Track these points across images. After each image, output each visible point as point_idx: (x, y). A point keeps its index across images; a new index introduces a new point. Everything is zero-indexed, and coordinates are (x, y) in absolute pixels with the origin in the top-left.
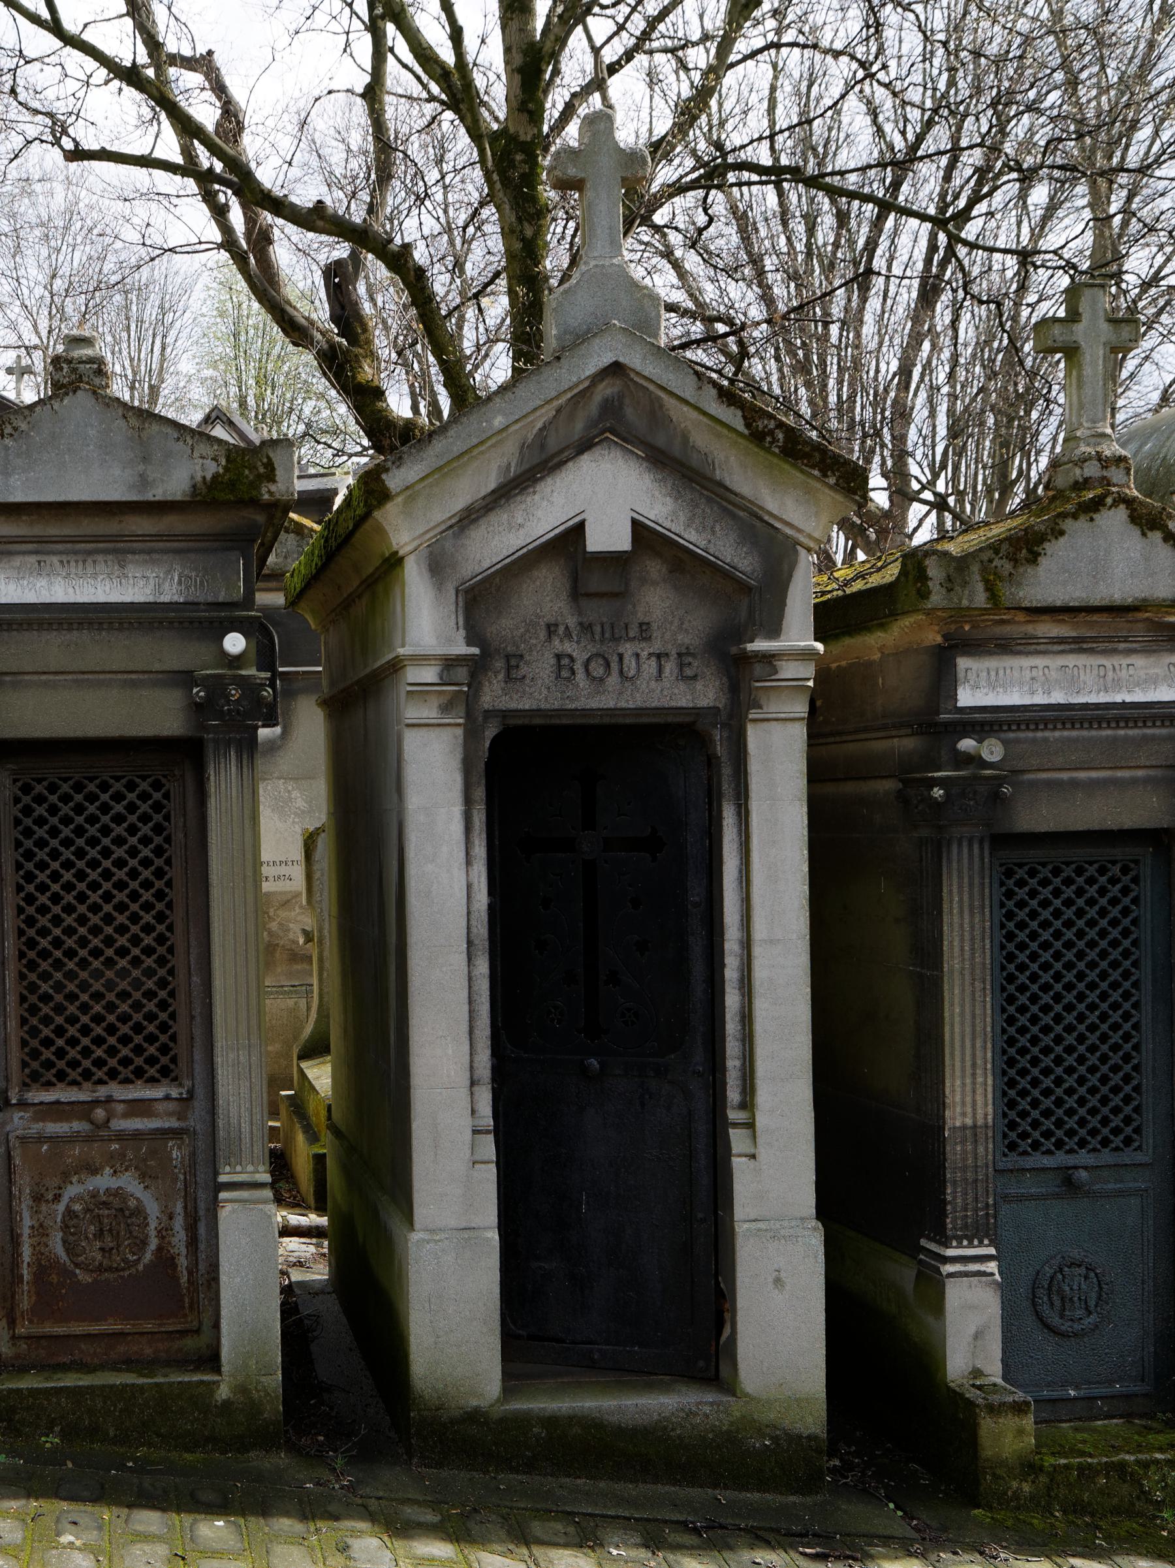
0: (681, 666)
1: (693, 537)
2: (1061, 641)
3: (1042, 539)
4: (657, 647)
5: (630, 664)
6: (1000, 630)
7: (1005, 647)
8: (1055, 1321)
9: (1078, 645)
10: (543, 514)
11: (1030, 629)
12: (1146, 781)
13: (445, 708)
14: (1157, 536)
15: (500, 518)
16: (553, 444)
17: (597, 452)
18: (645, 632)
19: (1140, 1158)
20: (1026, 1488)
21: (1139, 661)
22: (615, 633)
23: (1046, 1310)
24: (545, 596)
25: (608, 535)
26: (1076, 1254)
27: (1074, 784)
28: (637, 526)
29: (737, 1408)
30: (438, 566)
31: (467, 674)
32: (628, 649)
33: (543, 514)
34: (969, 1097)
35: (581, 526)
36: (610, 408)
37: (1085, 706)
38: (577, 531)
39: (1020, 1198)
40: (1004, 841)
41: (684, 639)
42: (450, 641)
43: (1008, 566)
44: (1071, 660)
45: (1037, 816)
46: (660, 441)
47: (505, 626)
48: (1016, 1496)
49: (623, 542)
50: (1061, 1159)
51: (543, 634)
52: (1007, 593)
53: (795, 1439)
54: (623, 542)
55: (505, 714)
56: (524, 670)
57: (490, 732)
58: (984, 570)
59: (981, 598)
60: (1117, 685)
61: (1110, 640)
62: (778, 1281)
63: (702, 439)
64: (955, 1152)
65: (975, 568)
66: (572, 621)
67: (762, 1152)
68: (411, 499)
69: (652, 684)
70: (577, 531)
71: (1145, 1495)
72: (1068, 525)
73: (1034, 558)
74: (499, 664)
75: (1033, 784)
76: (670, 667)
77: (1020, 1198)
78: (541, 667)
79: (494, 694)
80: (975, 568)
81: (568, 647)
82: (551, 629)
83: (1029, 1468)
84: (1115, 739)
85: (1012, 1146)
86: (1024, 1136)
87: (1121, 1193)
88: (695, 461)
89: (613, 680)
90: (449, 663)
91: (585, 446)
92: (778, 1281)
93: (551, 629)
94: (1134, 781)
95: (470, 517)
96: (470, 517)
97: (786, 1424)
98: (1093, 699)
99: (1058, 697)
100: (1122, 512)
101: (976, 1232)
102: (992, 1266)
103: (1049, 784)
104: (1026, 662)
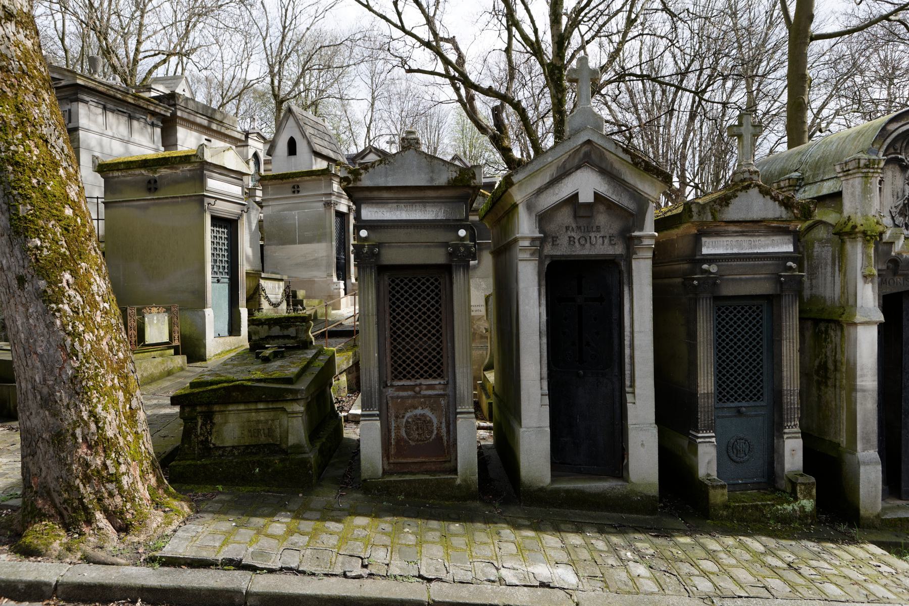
0: (610, 240)
1: (614, 198)
2: (736, 232)
3: (730, 198)
4: (602, 234)
5: (593, 240)
6: (716, 229)
7: (718, 234)
8: (735, 458)
9: (742, 234)
10: (565, 190)
11: (726, 228)
12: (765, 278)
13: (532, 254)
14: (768, 197)
15: (550, 191)
16: (568, 167)
17: (582, 169)
18: (598, 229)
19: (762, 403)
20: (725, 513)
21: (762, 239)
22: (588, 229)
23: (731, 454)
24: (565, 217)
25: (586, 197)
26: (741, 435)
27: (741, 279)
28: (596, 195)
29: (629, 487)
30: (529, 207)
31: (539, 243)
32: (593, 235)
33: (565, 190)
34: (706, 384)
35: (577, 194)
36: (587, 155)
37: (745, 254)
38: (576, 196)
39: (723, 417)
40: (717, 298)
41: (611, 231)
42: (534, 232)
43: (719, 207)
44: (740, 239)
45: (728, 290)
46: (603, 166)
47: (552, 227)
48: (721, 516)
49: (591, 199)
50: (736, 404)
51: (564, 230)
52: (720, 217)
53: (648, 497)
54: (591, 199)
55: (552, 256)
56: (558, 242)
57: (547, 263)
58: (711, 209)
59: (710, 218)
60: (755, 247)
61: (752, 232)
62: (642, 445)
63: (617, 165)
64: (701, 402)
65: (708, 208)
66: (574, 226)
67: (637, 402)
68: (521, 185)
69: (601, 246)
70: (576, 196)
71: (764, 516)
72: (739, 193)
73: (727, 205)
74: (550, 240)
75: (728, 279)
76: (606, 241)
77: (723, 417)
78: (564, 241)
79: (548, 250)
80: (708, 208)
81: (573, 234)
82: (567, 228)
83: (726, 506)
84: (754, 265)
85: (720, 400)
86: (724, 396)
87: (756, 415)
88: (615, 172)
89: (588, 245)
90: (533, 239)
91: (578, 167)
92: (642, 445)
93: (567, 228)
94: (761, 279)
95: (540, 191)
96: (540, 191)
97: (645, 492)
98: (747, 251)
99: (735, 251)
100: (757, 189)
101: (708, 428)
102: (714, 440)
103: (732, 279)
104: (725, 239)
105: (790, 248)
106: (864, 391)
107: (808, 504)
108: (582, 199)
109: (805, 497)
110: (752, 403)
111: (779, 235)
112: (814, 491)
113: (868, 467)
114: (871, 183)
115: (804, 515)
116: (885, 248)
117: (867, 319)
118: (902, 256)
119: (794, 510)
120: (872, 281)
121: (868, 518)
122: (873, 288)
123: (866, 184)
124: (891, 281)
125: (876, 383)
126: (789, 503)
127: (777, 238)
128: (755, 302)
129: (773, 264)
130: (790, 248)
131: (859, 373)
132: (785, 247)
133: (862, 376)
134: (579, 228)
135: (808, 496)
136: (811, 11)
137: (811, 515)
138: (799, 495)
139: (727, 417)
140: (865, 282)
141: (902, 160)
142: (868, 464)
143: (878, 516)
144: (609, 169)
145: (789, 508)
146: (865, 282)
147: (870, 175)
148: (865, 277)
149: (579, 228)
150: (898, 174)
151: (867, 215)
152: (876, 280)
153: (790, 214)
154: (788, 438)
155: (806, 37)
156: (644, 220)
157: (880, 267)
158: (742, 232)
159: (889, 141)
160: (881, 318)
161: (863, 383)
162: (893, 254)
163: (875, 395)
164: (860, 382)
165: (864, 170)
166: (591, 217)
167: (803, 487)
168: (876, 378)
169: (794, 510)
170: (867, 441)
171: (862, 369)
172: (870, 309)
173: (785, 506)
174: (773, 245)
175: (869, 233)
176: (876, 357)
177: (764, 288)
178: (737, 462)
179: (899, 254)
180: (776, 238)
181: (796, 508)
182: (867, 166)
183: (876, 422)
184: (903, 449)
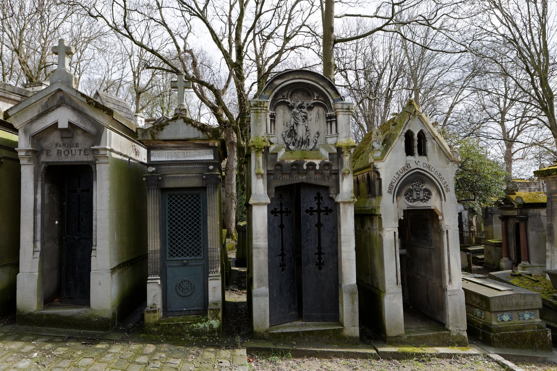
0: (85, 152)
1: (81, 125)
2: (174, 147)
3: (164, 125)
4: (79, 148)
5: (74, 152)
6: (159, 145)
7: (162, 148)
8: (181, 293)
9: (178, 148)
10: (49, 120)
11: (166, 145)
12: (195, 177)
13: (29, 161)
14: (190, 125)
15: (40, 121)
16: (50, 106)
17: (61, 108)
18: (77, 145)
19: (200, 258)
20: (156, 329)
21: (192, 151)
22: (71, 146)
23: (178, 291)
24: (55, 138)
25: (63, 125)
26: (186, 279)
27: (178, 177)
28: (70, 123)
30: (26, 132)
31: (35, 153)
32: (73, 149)
33: (49, 120)
34: (154, 244)
35: (57, 123)
36: (62, 98)
37: (180, 161)
38: (56, 124)
39: (172, 267)
40: (164, 190)
41: (86, 147)
42: (28, 147)
43: (156, 131)
44: (177, 151)
45: (169, 184)
46: (73, 105)
47: (46, 144)
48: (153, 331)
49: (66, 126)
50: (182, 258)
51: (55, 146)
52: (156, 137)
53: (103, 319)
54: (66, 126)
55: (47, 163)
56: (50, 153)
57: (43, 166)
58: (151, 132)
59: (150, 138)
60: (187, 156)
61: (185, 147)
62: (100, 284)
63: (80, 104)
64: (150, 256)
65: (149, 132)
66: (61, 143)
67: (98, 256)
68: (16, 117)
69: (77, 157)
70: (56, 124)
71: (184, 331)
72: (170, 123)
73: (162, 129)
74: (45, 152)
75: (169, 177)
76: (82, 153)
77: (172, 267)
78: (54, 153)
79: (44, 158)
80: (149, 132)
81: (60, 148)
82: (57, 145)
83: (157, 324)
84: (187, 168)
85: (172, 255)
86: (174, 253)
87: (196, 265)
88: (80, 109)
89: (70, 155)
90: (27, 151)
91: (58, 106)
92: (100, 284)
93: (57, 145)
94: (192, 177)
95: (32, 121)
96: (32, 121)
97: (101, 315)
98: (182, 159)
99: (174, 159)
100: (182, 120)
101: (155, 274)
102: (159, 281)
103: (173, 177)
104: (166, 152)
105: (211, 157)
106: (258, 248)
107: (215, 323)
108: (60, 126)
109: (213, 319)
110: (193, 257)
111: (204, 149)
112: (220, 315)
113: (259, 298)
114: (260, 116)
115: (213, 330)
116: (273, 156)
117: (257, 202)
118: (284, 162)
119: (205, 326)
120: (263, 179)
121: (260, 333)
122: (263, 182)
123: (257, 117)
124: (281, 178)
125: (266, 243)
126: (201, 323)
127: (202, 151)
128: (195, 192)
129: (200, 167)
130: (211, 157)
131: (254, 236)
132: (209, 156)
133: (256, 238)
134: (64, 144)
135: (216, 317)
136: (331, 25)
137: (218, 330)
138: (209, 317)
139: (175, 266)
140: (258, 178)
141: (289, 103)
142: (259, 296)
143: (267, 331)
144: (77, 107)
145: (201, 326)
146: (258, 178)
147: (259, 111)
148: (257, 174)
149: (64, 144)
150: (287, 111)
151: (258, 136)
152: (266, 176)
153: (205, 135)
154: (210, 280)
155: (331, 40)
156: (101, 139)
157: (269, 169)
158: (177, 147)
159: (276, 91)
160: (269, 201)
161: (257, 243)
162: (278, 160)
163: (266, 251)
164: (255, 243)
165: (254, 108)
166: (72, 137)
167: (211, 312)
168: (267, 240)
169: (205, 326)
170: (261, 281)
171: (257, 234)
172: (261, 195)
173: (199, 324)
174: (199, 155)
175: (256, 147)
176: (266, 226)
177: (195, 182)
178: (183, 296)
179: (282, 160)
180: (201, 151)
181: (206, 326)
182: (256, 106)
183: (267, 269)
184: (303, 288)
